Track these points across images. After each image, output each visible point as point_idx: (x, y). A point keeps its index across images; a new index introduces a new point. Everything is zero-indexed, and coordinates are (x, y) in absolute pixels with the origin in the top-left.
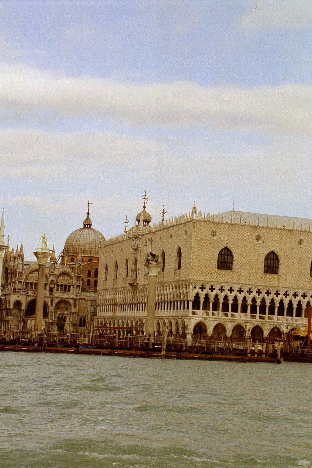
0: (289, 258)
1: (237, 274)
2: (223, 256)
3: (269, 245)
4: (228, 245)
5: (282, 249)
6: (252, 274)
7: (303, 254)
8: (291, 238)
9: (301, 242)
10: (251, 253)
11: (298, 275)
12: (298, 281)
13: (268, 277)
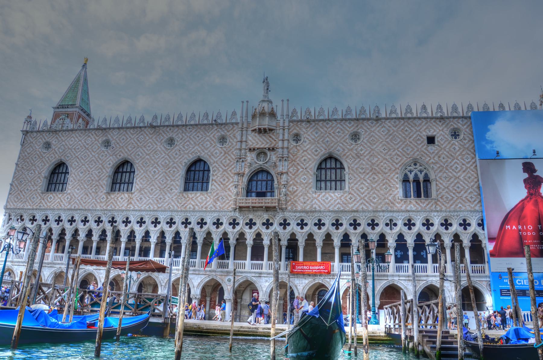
0: (149, 165)
1: (69, 196)
2: (60, 175)
3: (121, 151)
4: (62, 158)
5: (139, 155)
6: (89, 195)
7: (172, 157)
8: (155, 138)
9: (171, 142)
10: (92, 165)
11: (160, 191)
12: (160, 199)
13: (112, 196)
